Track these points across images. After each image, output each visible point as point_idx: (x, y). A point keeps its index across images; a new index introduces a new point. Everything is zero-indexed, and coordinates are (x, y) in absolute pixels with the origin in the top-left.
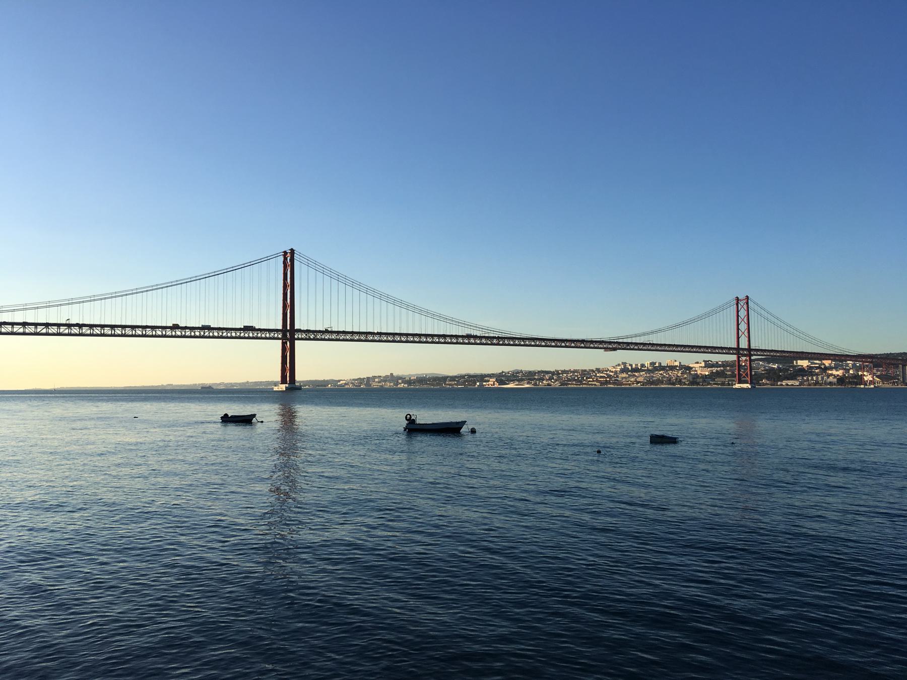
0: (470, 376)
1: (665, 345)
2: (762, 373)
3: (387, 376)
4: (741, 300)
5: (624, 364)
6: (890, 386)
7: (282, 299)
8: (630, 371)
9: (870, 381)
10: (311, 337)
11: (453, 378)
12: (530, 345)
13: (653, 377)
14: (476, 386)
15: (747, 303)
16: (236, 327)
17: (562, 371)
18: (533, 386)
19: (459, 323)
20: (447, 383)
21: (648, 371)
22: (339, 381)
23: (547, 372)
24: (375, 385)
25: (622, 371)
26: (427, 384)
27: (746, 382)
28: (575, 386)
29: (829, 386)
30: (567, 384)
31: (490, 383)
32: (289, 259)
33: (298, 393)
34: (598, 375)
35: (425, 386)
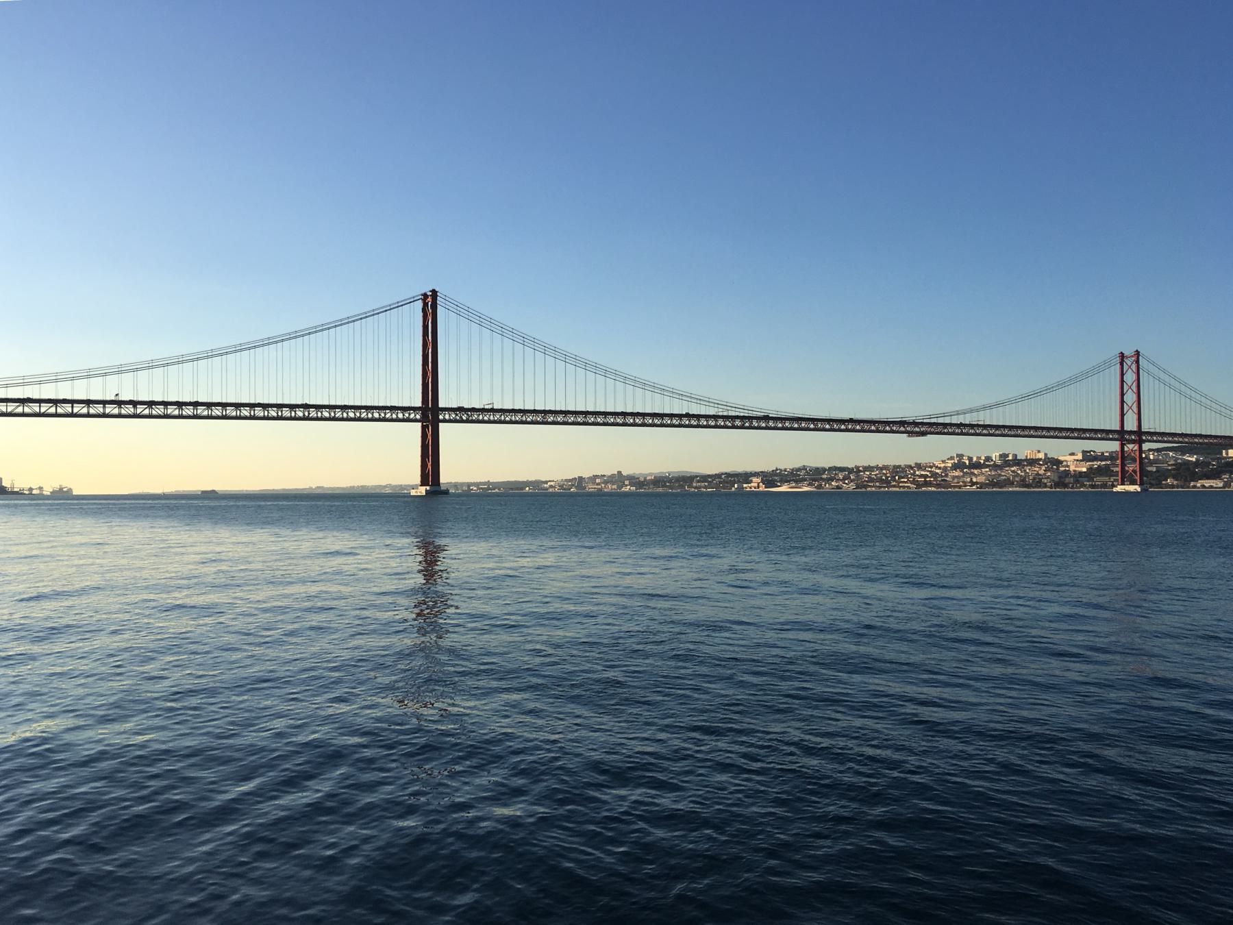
0: (728, 475)
4: (1127, 357)
5: (960, 456)
8: (967, 467)
10: (464, 418)
11: (704, 478)
13: (1000, 475)
14: (733, 489)
15: (1137, 362)
18: (815, 490)
19: (681, 396)
20: (694, 484)
21: (995, 467)
22: (546, 482)
23: (842, 469)
24: (591, 488)
25: (955, 467)
26: (666, 486)
27: (1133, 483)
30: (866, 487)
31: (753, 484)
32: (430, 303)
33: (444, 498)
34: (917, 473)
35: (660, 490)
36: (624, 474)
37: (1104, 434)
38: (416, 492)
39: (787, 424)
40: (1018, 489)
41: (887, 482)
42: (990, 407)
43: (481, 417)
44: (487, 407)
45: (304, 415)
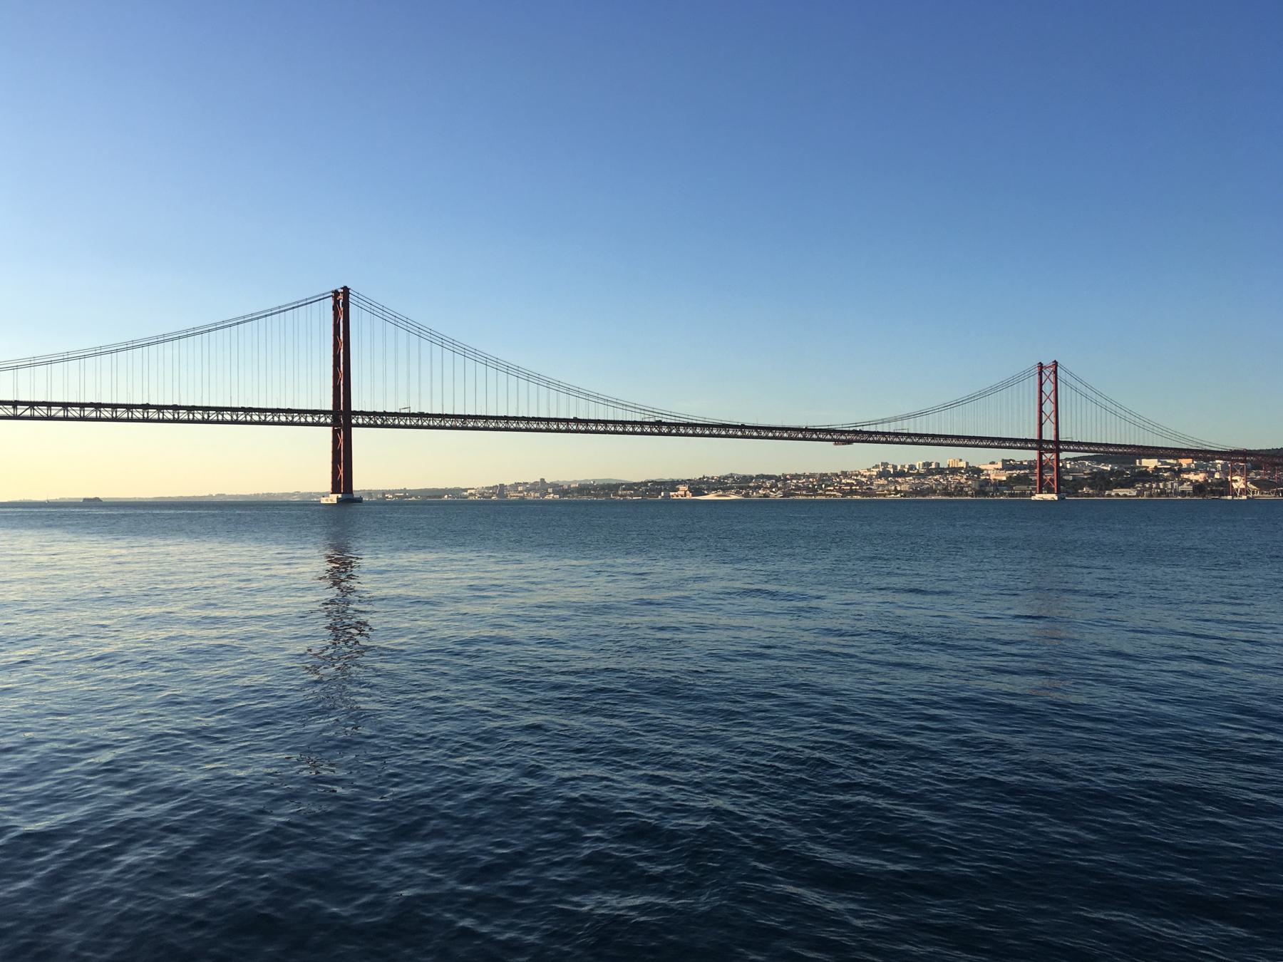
0: (655, 483)
1: (927, 435)
2: (1084, 479)
3: (536, 483)
4: (1046, 368)
5: (885, 464)
6: (1272, 497)
7: (332, 363)
8: (891, 476)
9: (1243, 489)
10: (379, 423)
11: (630, 486)
12: (703, 435)
13: (923, 484)
14: (660, 497)
15: (1055, 372)
16: (261, 407)
17: (790, 475)
19: (607, 401)
20: (620, 493)
21: (919, 475)
22: (466, 490)
23: (769, 477)
24: (513, 496)
25: (880, 475)
26: (592, 494)
27: (1050, 491)
28: (805, 498)
29: (1179, 498)
31: (679, 493)
32: (341, 301)
33: (357, 506)
34: (843, 481)
35: (585, 498)
36: (548, 481)
37: (1023, 443)
38: (327, 500)
39: (714, 431)
40: (940, 497)
41: (813, 491)
42: (915, 416)
43: (397, 422)
44: (403, 411)
45: (203, 418)
